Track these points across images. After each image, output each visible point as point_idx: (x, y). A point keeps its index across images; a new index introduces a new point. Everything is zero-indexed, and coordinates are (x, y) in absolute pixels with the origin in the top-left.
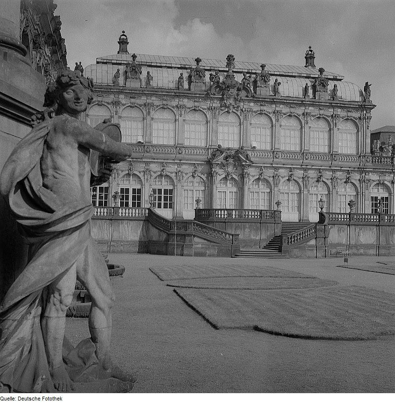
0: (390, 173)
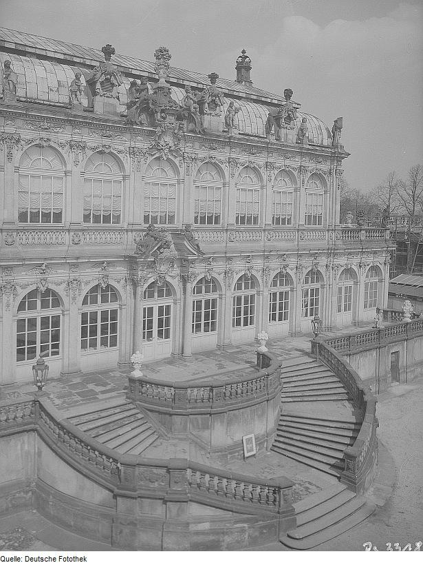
0: (357, 253)
